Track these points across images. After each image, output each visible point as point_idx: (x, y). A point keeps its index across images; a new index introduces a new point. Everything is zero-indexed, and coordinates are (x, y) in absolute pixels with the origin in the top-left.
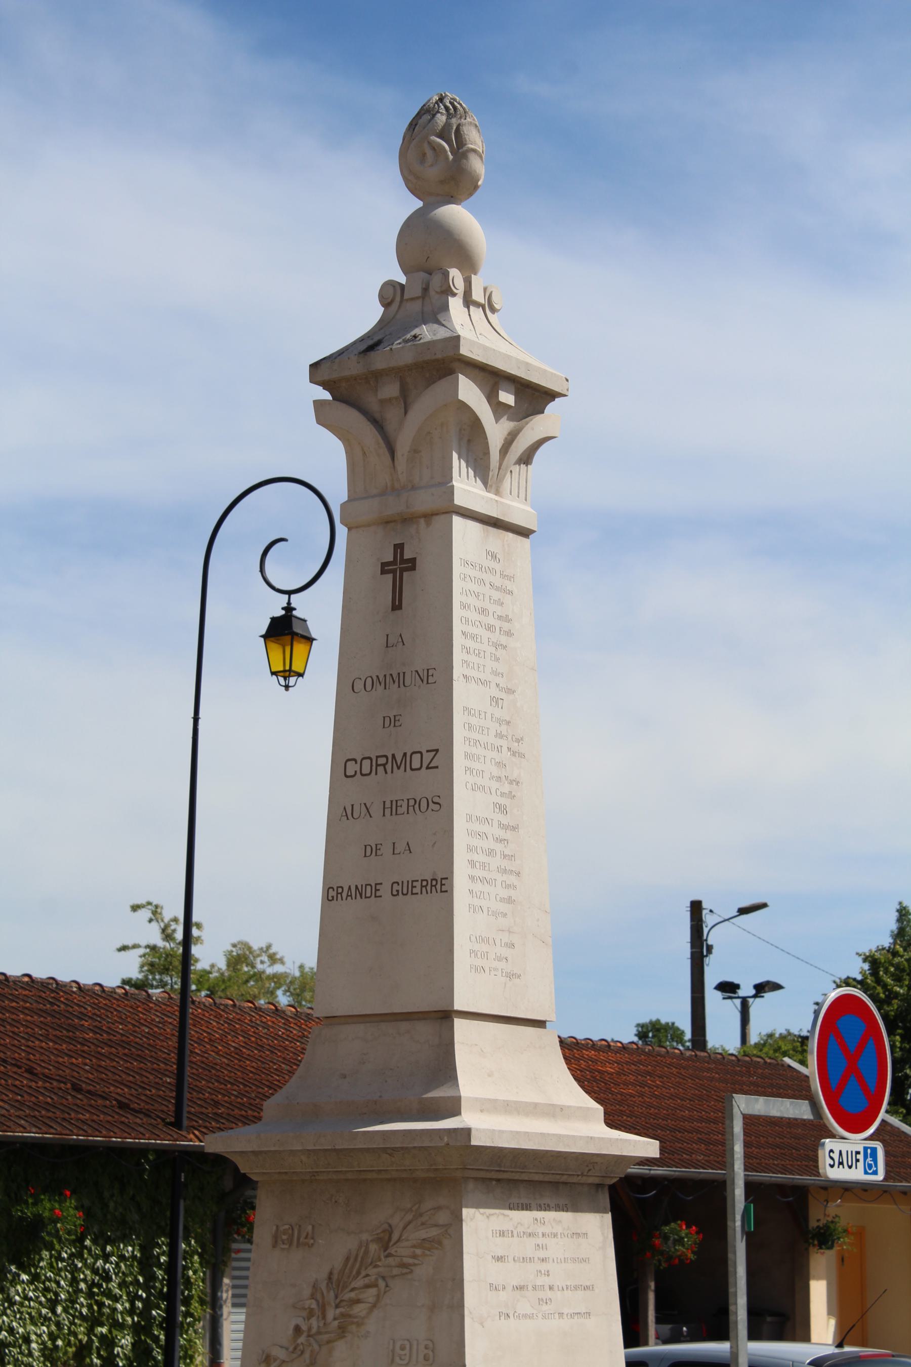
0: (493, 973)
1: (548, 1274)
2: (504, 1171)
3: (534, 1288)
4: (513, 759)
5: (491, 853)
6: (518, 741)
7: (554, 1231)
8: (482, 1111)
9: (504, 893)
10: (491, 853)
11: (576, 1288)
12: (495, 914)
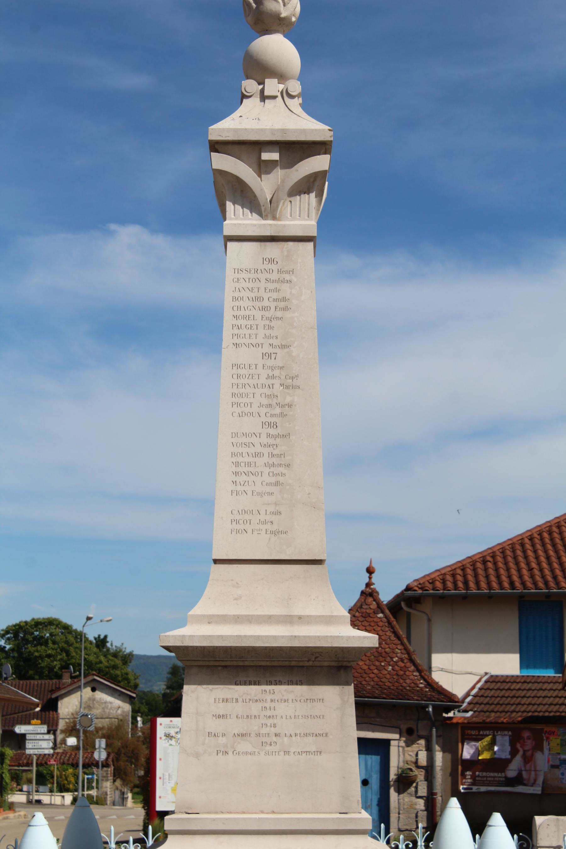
0: (255, 533)
1: (275, 726)
2: (226, 661)
3: (258, 735)
4: (287, 391)
5: (257, 455)
6: (292, 378)
7: (285, 698)
8: (209, 623)
9: (273, 480)
10: (257, 455)
11: (306, 735)
12: (260, 494)
